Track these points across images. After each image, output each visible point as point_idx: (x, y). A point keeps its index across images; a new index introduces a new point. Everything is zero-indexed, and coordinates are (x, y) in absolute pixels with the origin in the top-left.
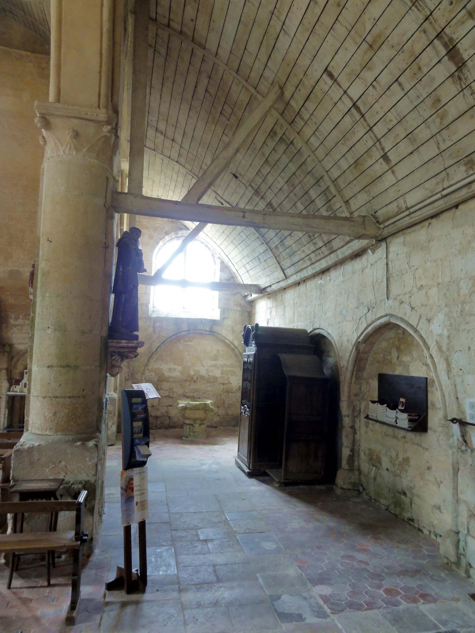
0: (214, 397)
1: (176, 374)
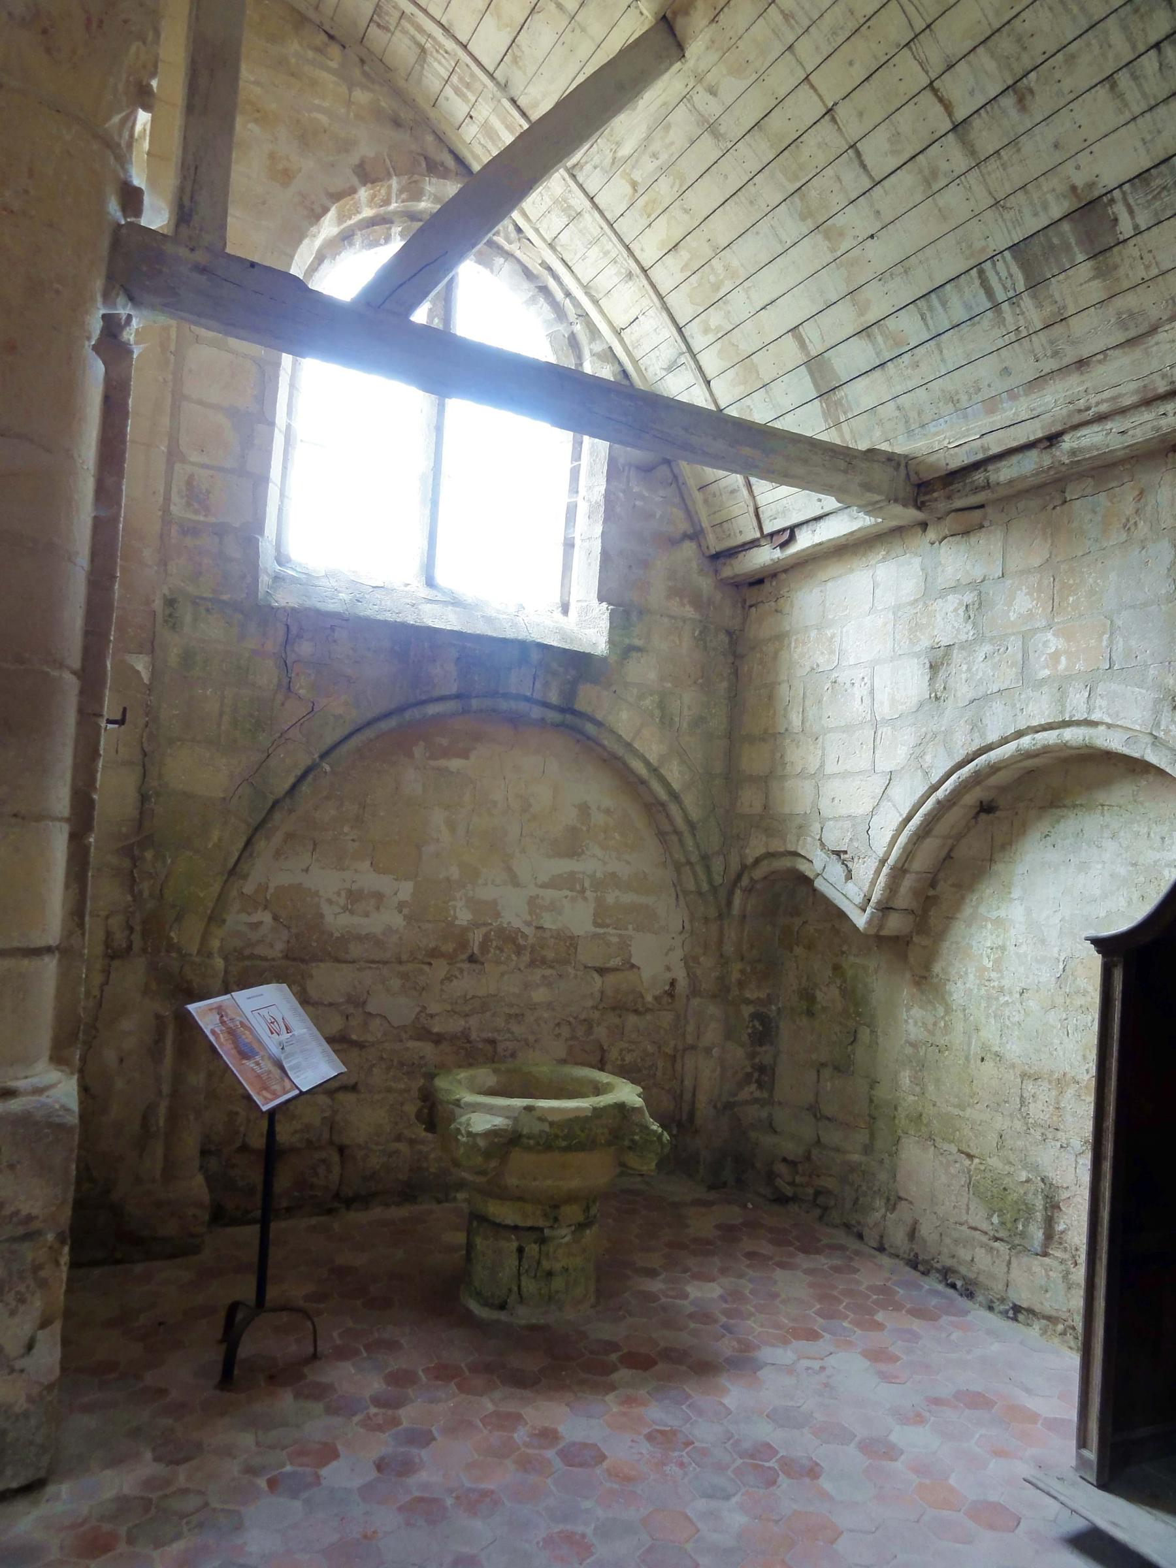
0: (558, 1036)
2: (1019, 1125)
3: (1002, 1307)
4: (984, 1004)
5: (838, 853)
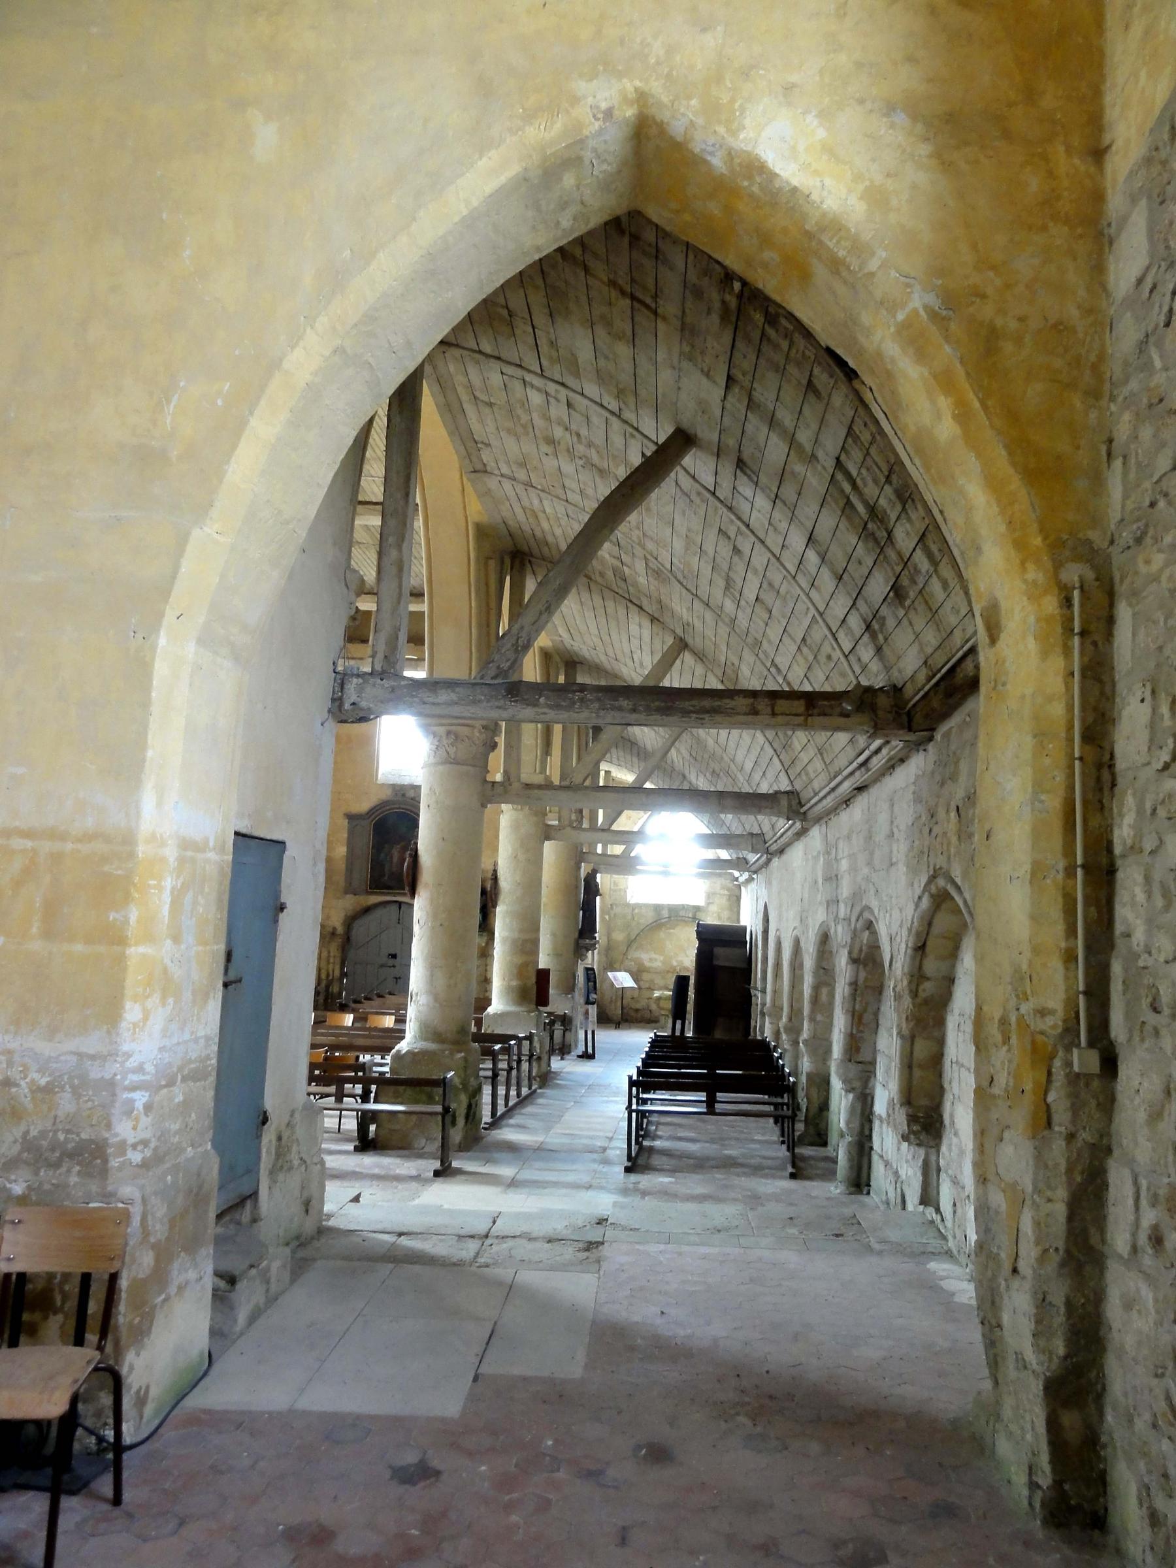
1: (657, 964)
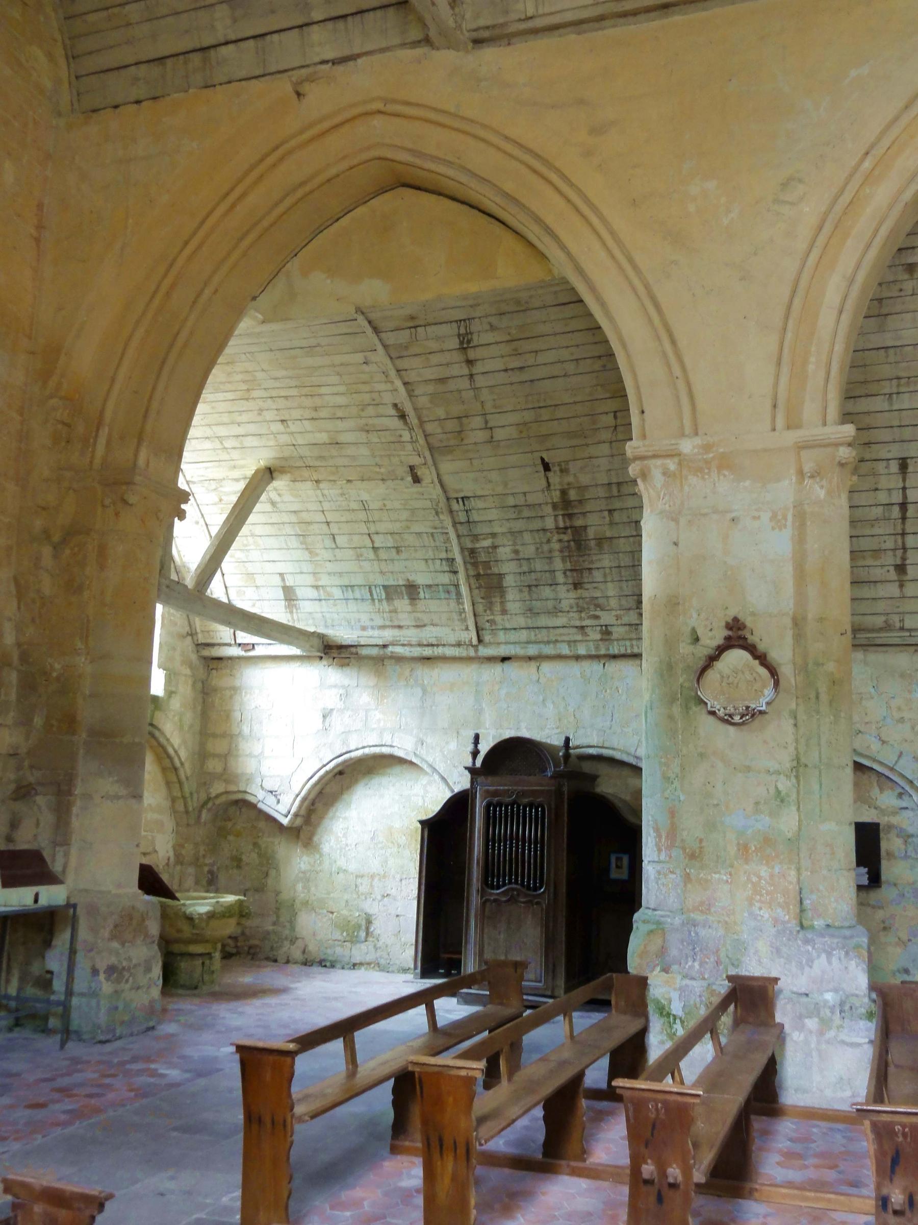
2: (355, 896)
3: (348, 966)
4: (338, 851)
5: (271, 792)
